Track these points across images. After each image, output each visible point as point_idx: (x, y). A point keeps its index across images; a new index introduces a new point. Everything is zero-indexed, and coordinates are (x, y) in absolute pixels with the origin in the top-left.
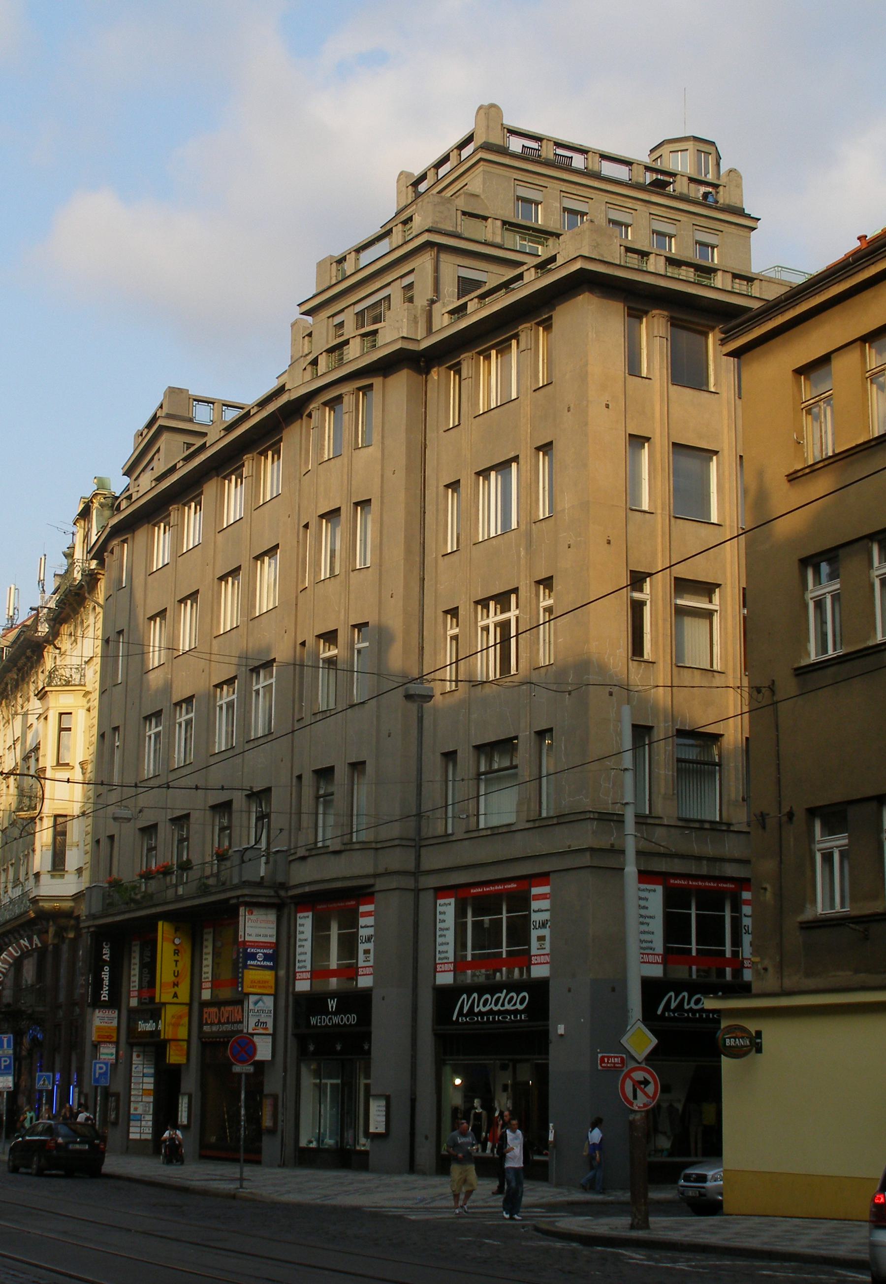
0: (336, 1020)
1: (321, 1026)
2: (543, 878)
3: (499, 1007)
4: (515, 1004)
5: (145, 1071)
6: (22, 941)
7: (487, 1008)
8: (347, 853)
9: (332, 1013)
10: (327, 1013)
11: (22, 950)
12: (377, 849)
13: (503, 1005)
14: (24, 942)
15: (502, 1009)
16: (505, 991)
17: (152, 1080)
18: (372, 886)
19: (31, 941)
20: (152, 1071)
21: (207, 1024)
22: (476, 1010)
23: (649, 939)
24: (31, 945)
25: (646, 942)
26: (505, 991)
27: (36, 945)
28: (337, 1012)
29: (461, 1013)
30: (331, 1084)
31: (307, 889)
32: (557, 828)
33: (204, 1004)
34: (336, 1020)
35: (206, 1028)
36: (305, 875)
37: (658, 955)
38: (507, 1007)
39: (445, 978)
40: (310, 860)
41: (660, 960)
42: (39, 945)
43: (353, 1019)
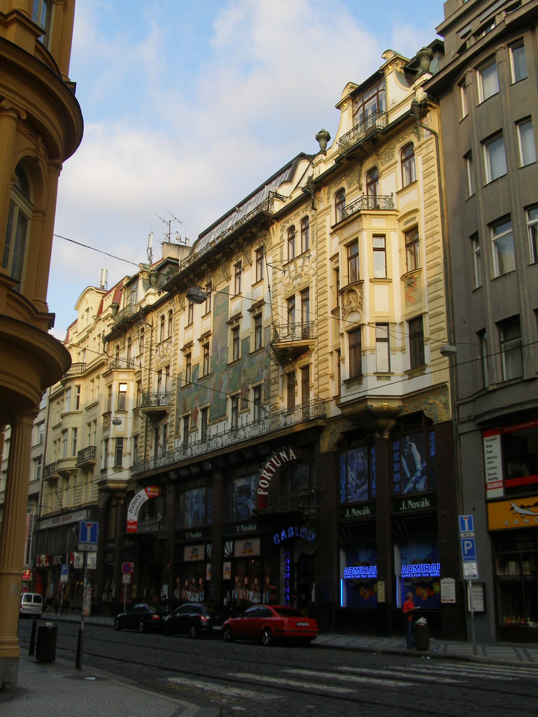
6: (281, 453)
11: (282, 461)
14: (283, 455)
19: (288, 454)
23: (494, 473)
24: (289, 457)
25: (492, 474)
27: (292, 457)
37: (500, 481)
41: (501, 485)
42: (295, 458)
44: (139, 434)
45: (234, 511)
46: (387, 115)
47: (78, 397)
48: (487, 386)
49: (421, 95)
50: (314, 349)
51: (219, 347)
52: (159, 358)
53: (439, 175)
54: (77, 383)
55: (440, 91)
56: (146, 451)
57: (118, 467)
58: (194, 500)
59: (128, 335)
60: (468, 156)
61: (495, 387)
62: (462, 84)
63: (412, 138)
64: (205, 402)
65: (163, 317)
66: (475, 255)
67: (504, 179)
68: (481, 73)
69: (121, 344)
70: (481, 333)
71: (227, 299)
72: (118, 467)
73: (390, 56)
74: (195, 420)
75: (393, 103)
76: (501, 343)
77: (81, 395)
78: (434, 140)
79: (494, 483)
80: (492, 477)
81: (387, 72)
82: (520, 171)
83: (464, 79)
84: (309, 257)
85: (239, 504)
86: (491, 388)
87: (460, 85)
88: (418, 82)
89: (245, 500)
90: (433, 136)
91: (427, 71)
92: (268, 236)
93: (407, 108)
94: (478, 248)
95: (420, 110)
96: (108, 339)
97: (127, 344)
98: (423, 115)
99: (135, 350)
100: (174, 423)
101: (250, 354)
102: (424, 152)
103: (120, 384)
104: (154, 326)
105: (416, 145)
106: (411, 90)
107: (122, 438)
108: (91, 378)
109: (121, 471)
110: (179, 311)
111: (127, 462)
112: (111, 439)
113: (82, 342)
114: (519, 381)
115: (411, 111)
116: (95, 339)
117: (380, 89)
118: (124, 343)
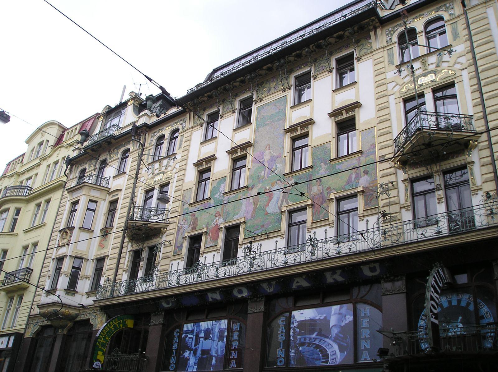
44: (108, 256)
45: (292, 354)
47: (16, 220)
50: (476, 146)
51: (267, 157)
52: (151, 176)
54: (18, 205)
56: (116, 275)
57: (72, 288)
58: (202, 335)
59: (102, 158)
64: (235, 217)
65: (162, 137)
69: (90, 166)
71: (282, 107)
72: (72, 288)
74: (216, 239)
77: (19, 218)
84: (450, 53)
85: (302, 344)
89: (315, 339)
92: (363, 42)
96: (71, 162)
97: (98, 166)
99: (110, 171)
100: (173, 243)
101: (331, 160)
103: (90, 201)
104: (147, 145)
107: (82, 259)
108: (38, 201)
109: (73, 295)
110: (193, 127)
111: (84, 285)
112: (68, 257)
113: (28, 171)
116: (49, 166)
118: (95, 165)
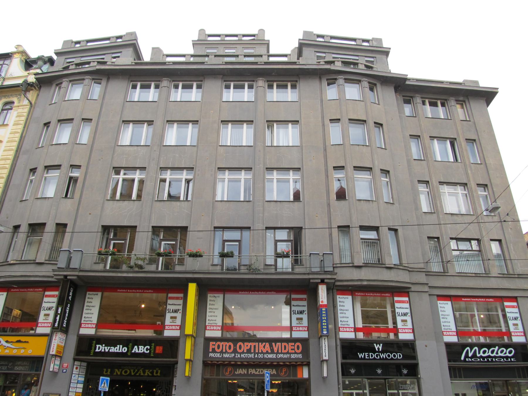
0: (383, 356)
1: (370, 359)
2: (514, 299)
3: (494, 354)
4: (505, 353)
5: (79, 379)
7: (486, 355)
8: (395, 270)
9: (379, 352)
10: (374, 351)
12: (409, 271)
13: (497, 353)
15: (497, 355)
16: (497, 347)
17: (81, 386)
18: (410, 288)
20: (83, 379)
21: (214, 351)
22: (478, 355)
26: (497, 347)
28: (383, 352)
29: (467, 356)
30: (356, 393)
31: (365, 283)
32: (517, 279)
33: (208, 340)
34: (383, 356)
35: (211, 355)
36: (346, 275)
38: (500, 354)
39: (454, 339)
40: (363, 269)
43: (399, 356)
46: (4, 79)
48: (9, 260)
49: (32, 79)
53: (24, 127)
55: (44, 82)
60: (47, 124)
61: (15, 262)
62: (59, 85)
63: (15, 100)
66: (29, 181)
67: (65, 145)
68: (72, 85)
70: (17, 228)
73: (20, 49)
75: (11, 75)
76: (27, 237)
78: (29, 107)
79: (299, 327)
80: (87, 319)
81: (15, 56)
82: (76, 145)
83: (61, 83)
86: (12, 262)
87: (57, 85)
88: (32, 71)
90: (29, 104)
91: (40, 68)
93: (20, 81)
94: (34, 177)
95: (27, 87)
98: (27, 90)
102: (20, 110)
105: (16, 104)
106: (26, 73)
114: (32, 262)
115: (22, 85)
117: (6, 62)
